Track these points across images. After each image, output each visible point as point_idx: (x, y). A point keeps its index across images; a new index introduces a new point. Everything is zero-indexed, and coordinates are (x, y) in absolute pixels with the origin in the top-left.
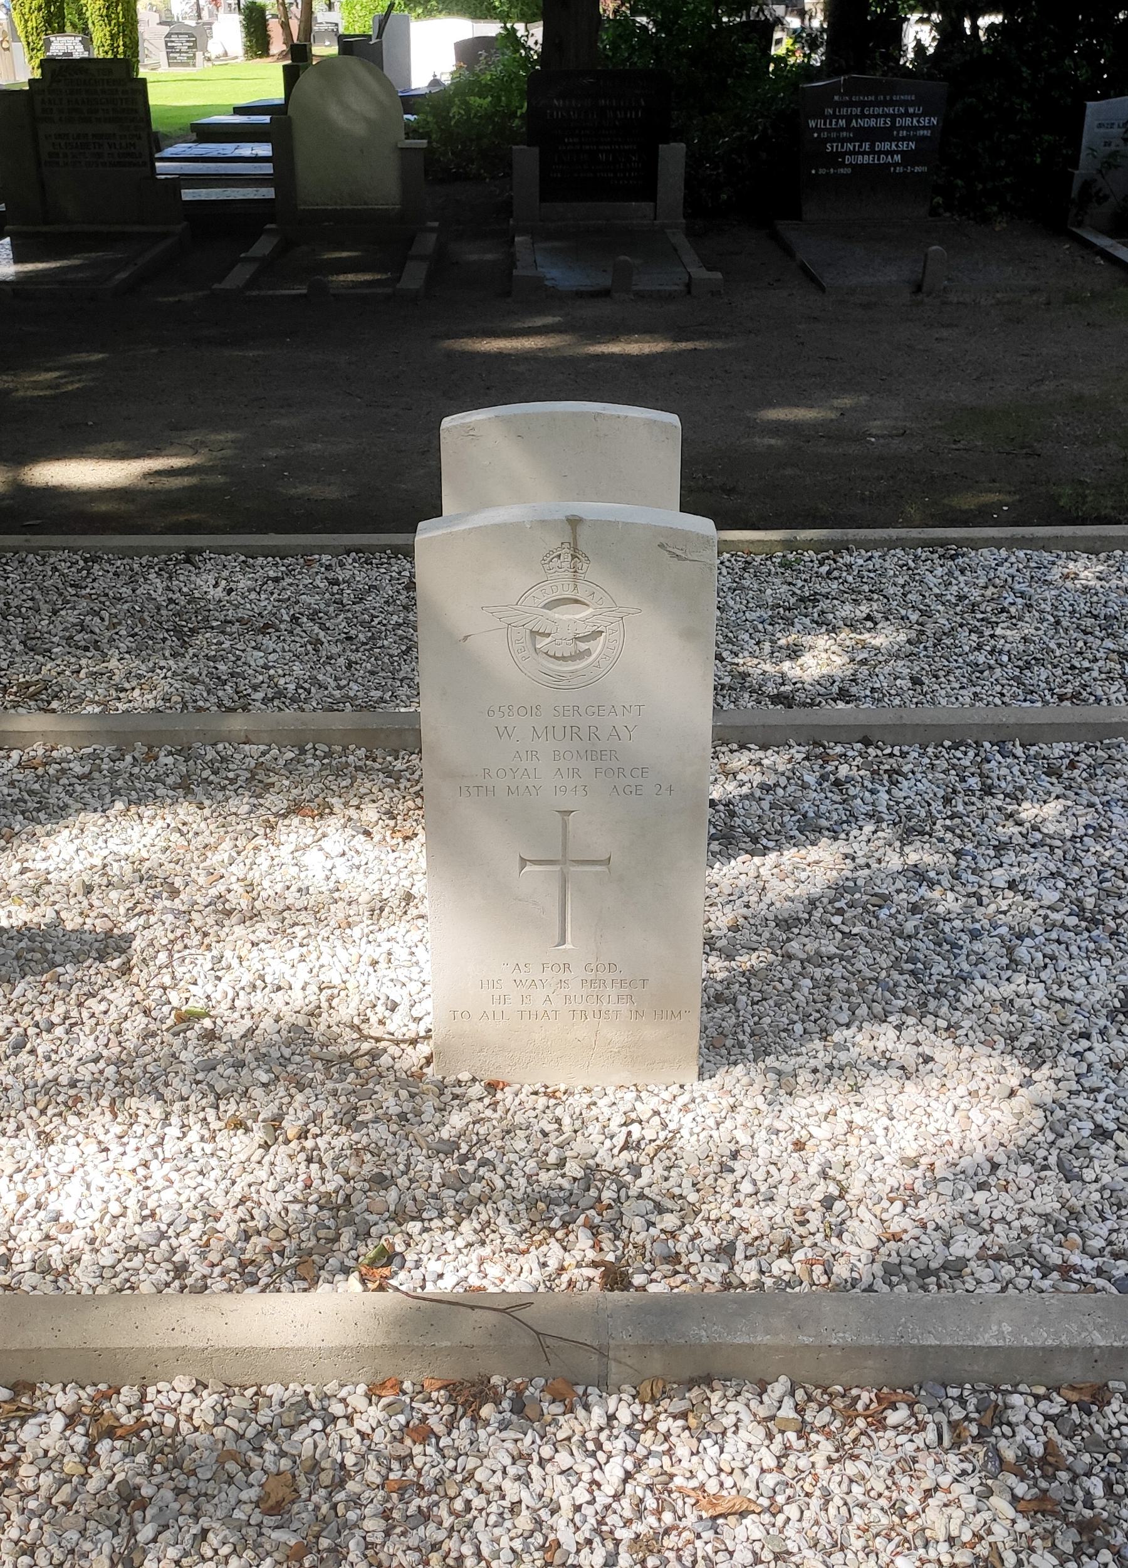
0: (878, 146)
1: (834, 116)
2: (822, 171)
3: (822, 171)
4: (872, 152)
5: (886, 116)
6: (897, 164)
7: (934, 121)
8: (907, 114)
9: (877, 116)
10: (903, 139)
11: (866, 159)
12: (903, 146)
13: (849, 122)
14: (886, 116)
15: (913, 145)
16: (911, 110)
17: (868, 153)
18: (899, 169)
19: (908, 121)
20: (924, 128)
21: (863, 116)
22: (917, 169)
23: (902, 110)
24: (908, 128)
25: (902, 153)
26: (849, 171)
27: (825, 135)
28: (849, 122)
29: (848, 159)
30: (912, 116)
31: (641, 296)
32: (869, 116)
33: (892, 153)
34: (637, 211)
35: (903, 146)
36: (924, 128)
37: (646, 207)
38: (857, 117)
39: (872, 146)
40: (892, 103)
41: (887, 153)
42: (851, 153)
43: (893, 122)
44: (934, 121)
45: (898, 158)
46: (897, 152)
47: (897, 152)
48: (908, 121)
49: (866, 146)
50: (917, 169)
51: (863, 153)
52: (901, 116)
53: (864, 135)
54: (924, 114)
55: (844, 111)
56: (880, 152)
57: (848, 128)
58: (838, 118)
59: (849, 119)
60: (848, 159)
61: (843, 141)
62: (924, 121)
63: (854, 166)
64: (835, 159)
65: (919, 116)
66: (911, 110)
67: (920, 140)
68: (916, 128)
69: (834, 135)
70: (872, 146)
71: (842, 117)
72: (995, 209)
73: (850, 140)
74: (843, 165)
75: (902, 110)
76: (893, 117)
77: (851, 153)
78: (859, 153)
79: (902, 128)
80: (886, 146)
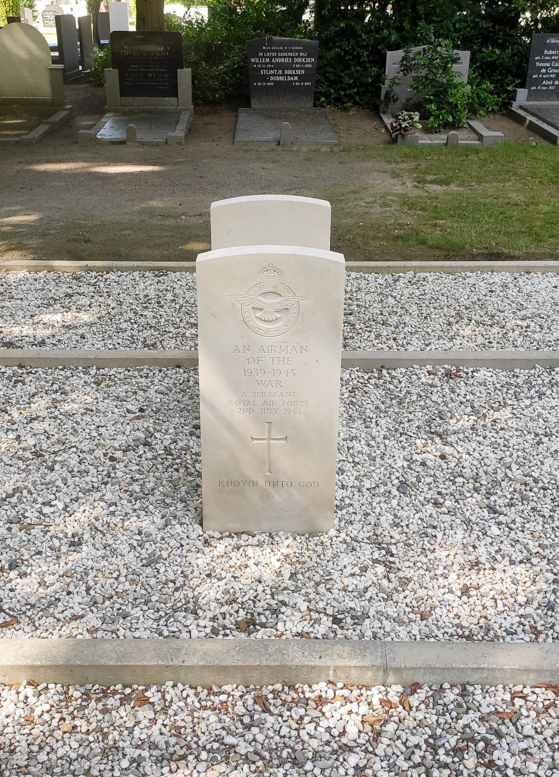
0: (286, 72)
1: (263, 57)
2: (259, 84)
3: (259, 84)
4: (283, 75)
6: (296, 81)
7: (313, 60)
8: (299, 56)
9: (285, 57)
10: (298, 69)
11: (281, 79)
12: (298, 72)
13: (271, 60)
14: (289, 57)
15: (303, 72)
16: (301, 54)
17: (282, 75)
18: (297, 84)
19: (300, 60)
20: (308, 63)
21: (278, 57)
22: (306, 84)
23: (297, 54)
24: (300, 63)
25: (298, 75)
26: (273, 84)
27: (259, 66)
28: (271, 60)
29: (272, 78)
30: (302, 57)
31: (142, 144)
32: (281, 57)
34: (168, 102)
35: (298, 72)
36: (308, 63)
37: (174, 100)
38: (274, 57)
39: (283, 72)
40: (291, 51)
41: (291, 75)
42: (273, 75)
43: (293, 60)
44: (313, 60)
46: (296, 75)
47: (296, 75)
48: (300, 60)
49: (280, 72)
50: (306, 84)
51: (279, 75)
52: (296, 57)
53: (279, 66)
54: (307, 57)
55: (268, 54)
56: (287, 75)
57: (271, 63)
58: (265, 57)
59: (271, 58)
60: (272, 78)
61: (269, 69)
62: (308, 60)
64: (265, 78)
65: (305, 57)
66: (301, 54)
67: (306, 69)
68: (304, 64)
69: (264, 66)
70: (283, 72)
71: (268, 57)
72: (350, 104)
73: (272, 69)
74: (269, 81)
75: (297, 54)
76: (293, 58)
77: (273, 75)
78: (277, 75)
79: (297, 63)
80: (290, 72)
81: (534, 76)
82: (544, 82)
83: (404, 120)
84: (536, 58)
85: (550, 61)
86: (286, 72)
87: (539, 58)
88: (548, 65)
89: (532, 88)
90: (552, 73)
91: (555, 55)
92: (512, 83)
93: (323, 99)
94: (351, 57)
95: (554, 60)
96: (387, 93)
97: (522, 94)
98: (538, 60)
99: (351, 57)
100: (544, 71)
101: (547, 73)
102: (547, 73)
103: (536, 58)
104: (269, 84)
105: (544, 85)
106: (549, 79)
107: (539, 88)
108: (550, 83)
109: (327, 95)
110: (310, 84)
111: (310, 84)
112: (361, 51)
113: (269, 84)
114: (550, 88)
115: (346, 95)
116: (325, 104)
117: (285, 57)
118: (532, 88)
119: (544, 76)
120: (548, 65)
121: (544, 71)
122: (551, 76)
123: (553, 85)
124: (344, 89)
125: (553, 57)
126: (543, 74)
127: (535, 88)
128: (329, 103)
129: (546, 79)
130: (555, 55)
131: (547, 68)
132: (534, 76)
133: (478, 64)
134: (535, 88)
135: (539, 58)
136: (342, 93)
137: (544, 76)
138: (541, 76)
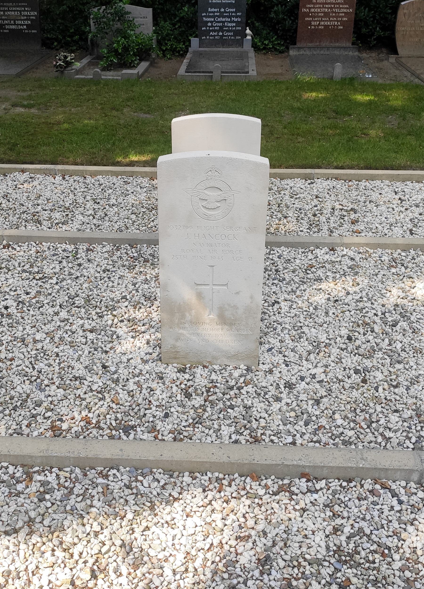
0: (17, 22)
4: (15, 24)
5: (18, 11)
6: (25, 29)
7: (36, 13)
8: (25, 11)
9: (14, 11)
11: (14, 27)
12: (26, 22)
14: (18, 11)
16: (26, 9)
17: (14, 25)
18: (26, 31)
19: (26, 13)
20: (32, 16)
21: (9, 11)
22: (33, 31)
24: (27, 16)
25: (26, 25)
29: (7, 27)
30: (27, 11)
32: (11, 11)
33: (23, 25)
35: (26, 22)
36: (32, 16)
38: (7, 11)
39: (15, 22)
40: (18, 6)
41: (21, 25)
42: (8, 24)
44: (36, 13)
45: (25, 27)
46: (25, 25)
47: (25, 25)
48: (26, 13)
49: (12, 22)
50: (33, 31)
51: (12, 25)
52: (23, 11)
54: (32, 11)
56: (18, 25)
57: (4, 15)
60: (7, 27)
62: (32, 13)
63: (9, 29)
65: (29, 11)
66: (26, 9)
67: (32, 20)
68: (30, 16)
73: (6, 20)
74: (5, 29)
75: (23, 9)
76: (20, 11)
77: (8, 24)
78: (10, 25)
79: (24, 16)
80: (20, 22)
81: (203, 29)
82: (211, 33)
83: (60, 60)
84: (203, 15)
85: (214, 17)
86: (17, 22)
87: (205, 14)
88: (213, 20)
89: (203, 38)
90: (217, 26)
91: (217, 12)
92: (194, 33)
93: (56, 44)
94: (77, 12)
95: (217, 16)
96: (92, 40)
97: (195, 42)
98: (204, 16)
99: (77, 12)
100: (210, 24)
101: (212, 26)
102: (212, 26)
103: (203, 15)
104: (5, 31)
105: (212, 36)
106: (214, 31)
107: (208, 37)
108: (216, 34)
109: (59, 42)
110: (36, 31)
111: (36, 31)
112: (82, 8)
113: (5, 31)
114: (216, 37)
115: (73, 41)
116: (58, 47)
117: (14, 11)
118: (203, 38)
119: (211, 29)
120: (213, 20)
121: (210, 24)
122: (216, 28)
123: (218, 35)
124: (70, 36)
125: (216, 14)
126: (210, 27)
127: (205, 38)
128: (62, 47)
129: (212, 31)
130: (217, 12)
131: (211, 22)
132: (203, 29)
133: (178, 19)
134: (205, 38)
135: (205, 14)
136: (69, 39)
137: (211, 29)
138: (208, 28)
